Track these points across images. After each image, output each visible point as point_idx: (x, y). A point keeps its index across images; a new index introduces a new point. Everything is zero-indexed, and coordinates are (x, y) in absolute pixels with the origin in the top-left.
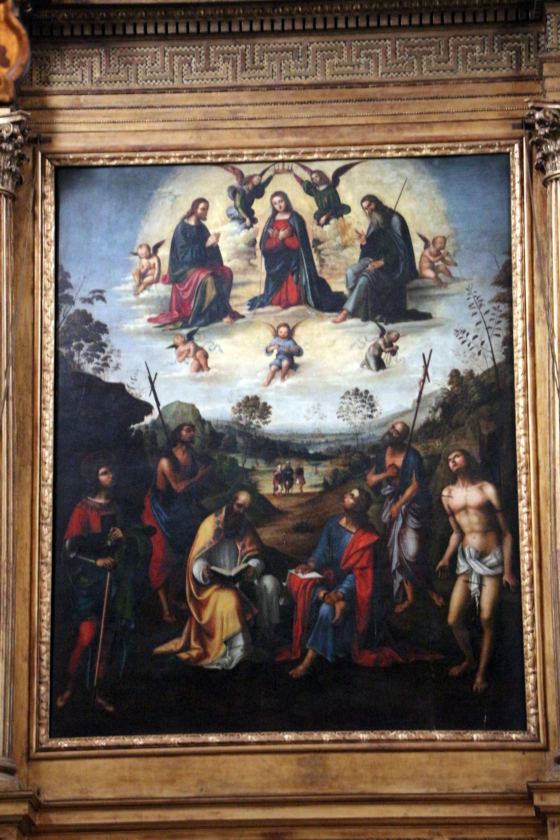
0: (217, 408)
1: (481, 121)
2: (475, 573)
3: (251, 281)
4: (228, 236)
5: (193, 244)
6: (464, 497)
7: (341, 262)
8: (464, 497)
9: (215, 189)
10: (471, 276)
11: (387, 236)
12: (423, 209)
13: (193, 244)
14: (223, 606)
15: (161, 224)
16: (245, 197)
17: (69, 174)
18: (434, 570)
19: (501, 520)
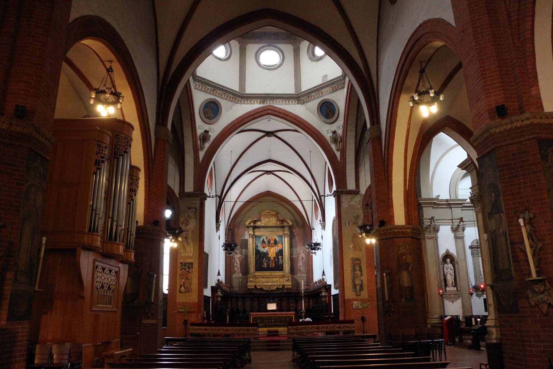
0: (265, 251)
1: (281, 234)
2: (281, 262)
3: (267, 243)
4: (265, 240)
5: (263, 241)
6: (280, 257)
7: (272, 242)
8: (280, 257)
9: (265, 237)
10: (281, 243)
11: (275, 241)
12: (278, 239)
13: (263, 241)
14: (265, 264)
15: (261, 240)
16: (267, 238)
17: (256, 236)
18: (278, 262)
19: (282, 258)
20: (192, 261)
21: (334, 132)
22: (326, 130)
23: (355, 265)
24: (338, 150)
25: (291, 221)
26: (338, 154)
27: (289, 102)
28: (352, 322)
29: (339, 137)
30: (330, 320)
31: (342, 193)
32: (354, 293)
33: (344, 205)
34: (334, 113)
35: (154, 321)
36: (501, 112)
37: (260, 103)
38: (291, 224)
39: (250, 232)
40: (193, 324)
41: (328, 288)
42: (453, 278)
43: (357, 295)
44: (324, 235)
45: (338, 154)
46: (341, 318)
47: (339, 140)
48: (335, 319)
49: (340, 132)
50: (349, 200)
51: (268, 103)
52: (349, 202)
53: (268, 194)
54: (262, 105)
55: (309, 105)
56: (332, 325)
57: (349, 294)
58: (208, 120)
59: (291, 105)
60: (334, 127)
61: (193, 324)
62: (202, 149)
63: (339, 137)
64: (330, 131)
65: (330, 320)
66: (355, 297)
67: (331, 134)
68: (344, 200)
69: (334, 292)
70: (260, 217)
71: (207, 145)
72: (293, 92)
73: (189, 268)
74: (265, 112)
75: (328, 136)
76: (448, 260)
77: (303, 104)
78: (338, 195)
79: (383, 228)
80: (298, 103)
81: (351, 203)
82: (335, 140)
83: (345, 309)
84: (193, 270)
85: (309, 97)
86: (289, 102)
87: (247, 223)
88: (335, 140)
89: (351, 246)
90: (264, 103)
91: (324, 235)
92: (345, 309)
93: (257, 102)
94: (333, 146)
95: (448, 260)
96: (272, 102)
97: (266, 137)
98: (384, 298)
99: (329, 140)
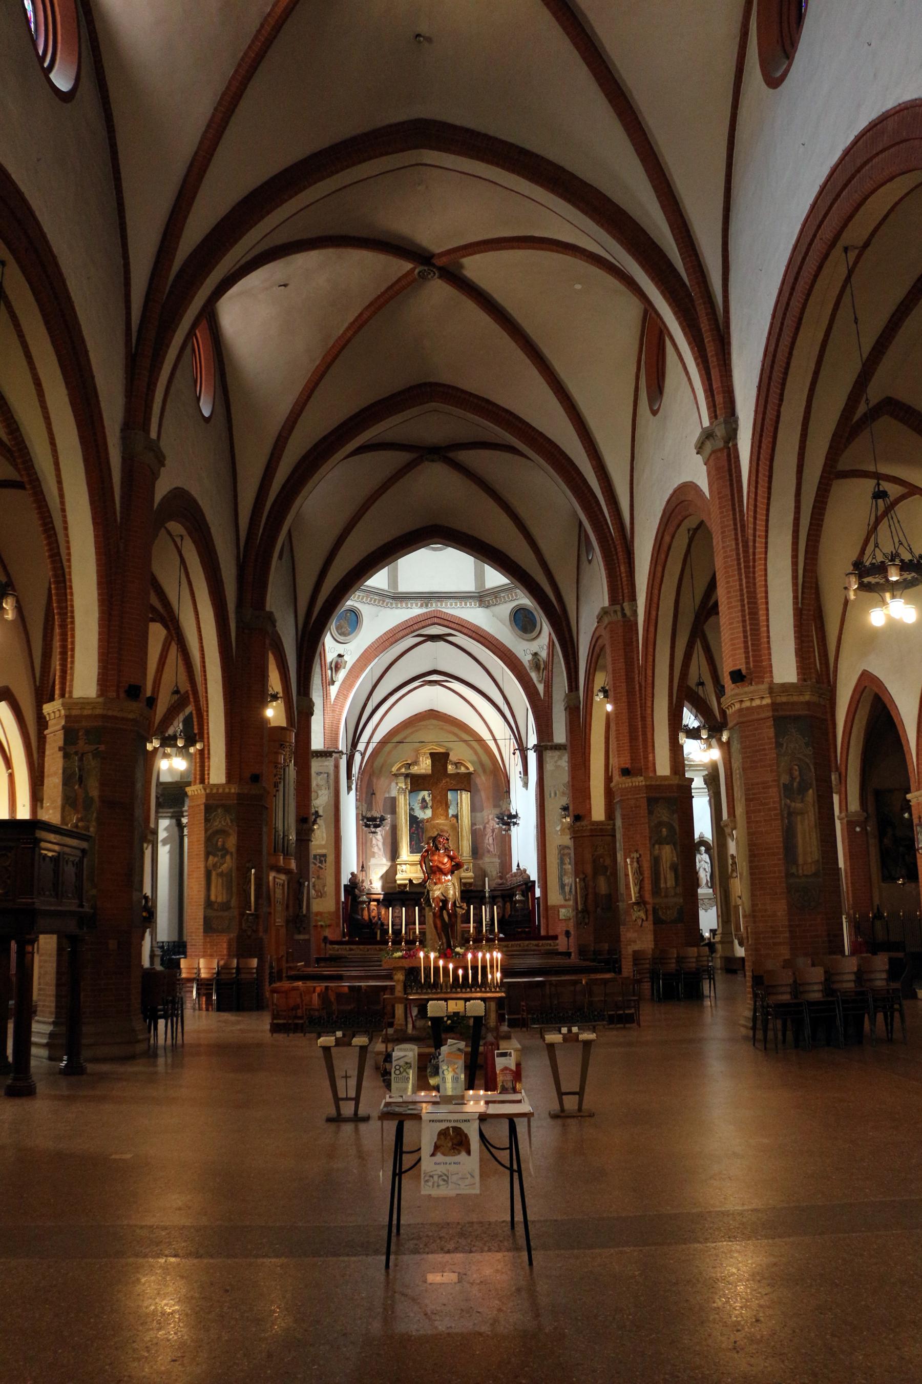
20: (323, 851)
21: (535, 654)
22: (524, 650)
23: (564, 855)
24: (540, 682)
25: (472, 763)
26: (541, 688)
27: (466, 604)
28: (555, 938)
29: (542, 663)
30: (524, 935)
31: (546, 748)
32: (561, 897)
33: (549, 767)
34: (535, 626)
35: (306, 937)
36: (626, 772)
37: (422, 606)
38: (471, 769)
39: (400, 785)
40: (332, 943)
41: (529, 886)
42: (708, 875)
43: (566, 900)
44: (523, 801)
45: (541, 688)
46: (543, 933)
47: (542, 666)
48: (533, 934)
49: (544, 654)
50: (556, 758)
51: (434, 606)
52: (556, 762)
53: (432, 715)
54: (424, 610)
55: (497, 609)
56: (527, 942)
57: (555, 898)
58: (343, 638)
59: (469, 610)
60: (534, 646)
61: (332, 943)
62: (333, 682)
63: (542, 663)
64: (528, 652)
65: (524, 935)
66: (563, 902)
67: (530, 657)
68: (548, 759)
69: (538, 893)
70: (417, 757)
71: (342, 675)
72: (473, 589)
73: (321, 862)
74: (429, 622)
75: (526, 659)
76: (703, 849)
77: (487, 607)
78: (539, 749)
79: (578, 824)
80: (480, 606)
81: (559, 763)
82: (537, 667)
83: (547, 919)
84: (328, 864)
85: (496, 597)
86: (466, 604)
87: (394, 769)
88: (537, 667)
89: (558, 828)
90: (427, 606)
91: (523, 801)
92: (547, 919)
93: (417, 605)
94: (534, 675)
95: (703, 849)
96: (439, 604)
97: (429, 643)
98: (577, 909)
99: (526, 664)
